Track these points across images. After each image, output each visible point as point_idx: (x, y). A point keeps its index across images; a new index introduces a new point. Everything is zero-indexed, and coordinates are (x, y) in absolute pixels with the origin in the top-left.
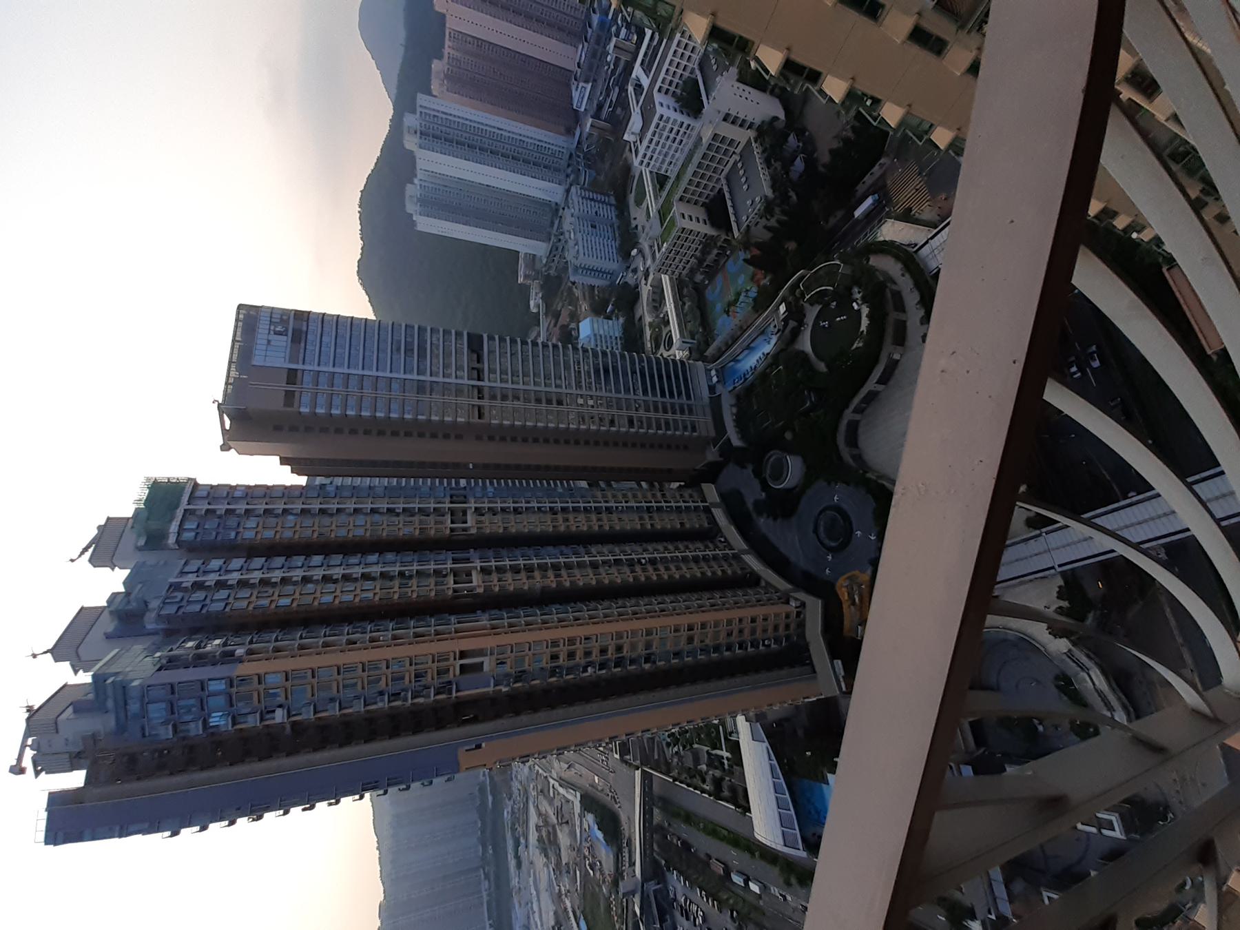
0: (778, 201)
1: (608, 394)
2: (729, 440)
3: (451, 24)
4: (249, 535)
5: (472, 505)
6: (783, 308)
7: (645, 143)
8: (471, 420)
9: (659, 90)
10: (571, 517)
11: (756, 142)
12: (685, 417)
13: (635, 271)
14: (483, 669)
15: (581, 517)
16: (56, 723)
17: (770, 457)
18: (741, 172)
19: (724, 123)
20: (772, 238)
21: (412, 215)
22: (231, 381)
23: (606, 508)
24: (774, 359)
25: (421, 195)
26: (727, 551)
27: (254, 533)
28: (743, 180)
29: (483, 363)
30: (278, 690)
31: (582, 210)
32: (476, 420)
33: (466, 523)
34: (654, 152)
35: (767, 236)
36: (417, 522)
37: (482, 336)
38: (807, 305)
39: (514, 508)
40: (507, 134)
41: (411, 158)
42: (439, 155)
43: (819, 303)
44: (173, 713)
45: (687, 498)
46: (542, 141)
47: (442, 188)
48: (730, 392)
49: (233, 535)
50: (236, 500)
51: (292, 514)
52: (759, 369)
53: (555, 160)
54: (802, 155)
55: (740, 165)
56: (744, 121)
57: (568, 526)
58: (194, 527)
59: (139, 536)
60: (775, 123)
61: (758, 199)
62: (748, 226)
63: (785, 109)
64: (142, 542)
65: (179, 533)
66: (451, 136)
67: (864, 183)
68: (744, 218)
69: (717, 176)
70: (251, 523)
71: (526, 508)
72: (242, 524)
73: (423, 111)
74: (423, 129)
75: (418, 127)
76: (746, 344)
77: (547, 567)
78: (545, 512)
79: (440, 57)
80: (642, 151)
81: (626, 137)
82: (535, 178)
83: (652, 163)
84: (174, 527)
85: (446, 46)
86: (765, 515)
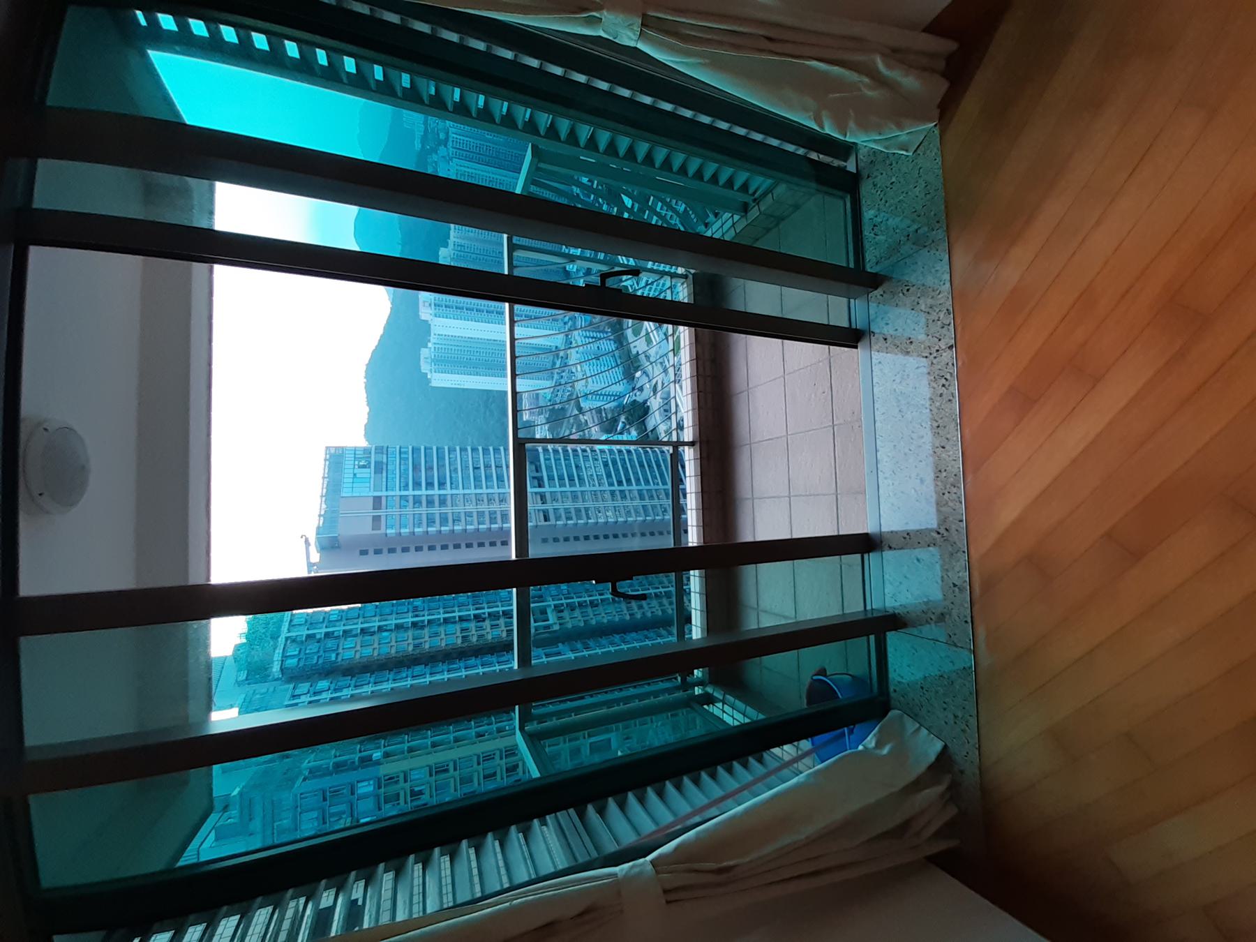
1: (656, 487)
4: (349, 655)
8: (539, 524)
13: (641, 389)
14: (610, 747)
16: (198, 851)
21: (427, 374)
22: (323, 513)
25: (435, 356)
27: (353, 652)
30: (423, 787)
36: (503, 625)
41: (426, 326)
42: (452, 320)
44: (324, 823)
49: (333, 656)
51: (386, 631)
58: (296, 653)
59: (239, 670)
64: (243, 676)
65: (282, 661)
66: (461, 305)
70: (349, 643)
72: (341, 645)
74: (436, 302)
75: (433, 301)
79: (446, 246)
82: (537, 328)
84: (277, 656)
85: (451, 237)
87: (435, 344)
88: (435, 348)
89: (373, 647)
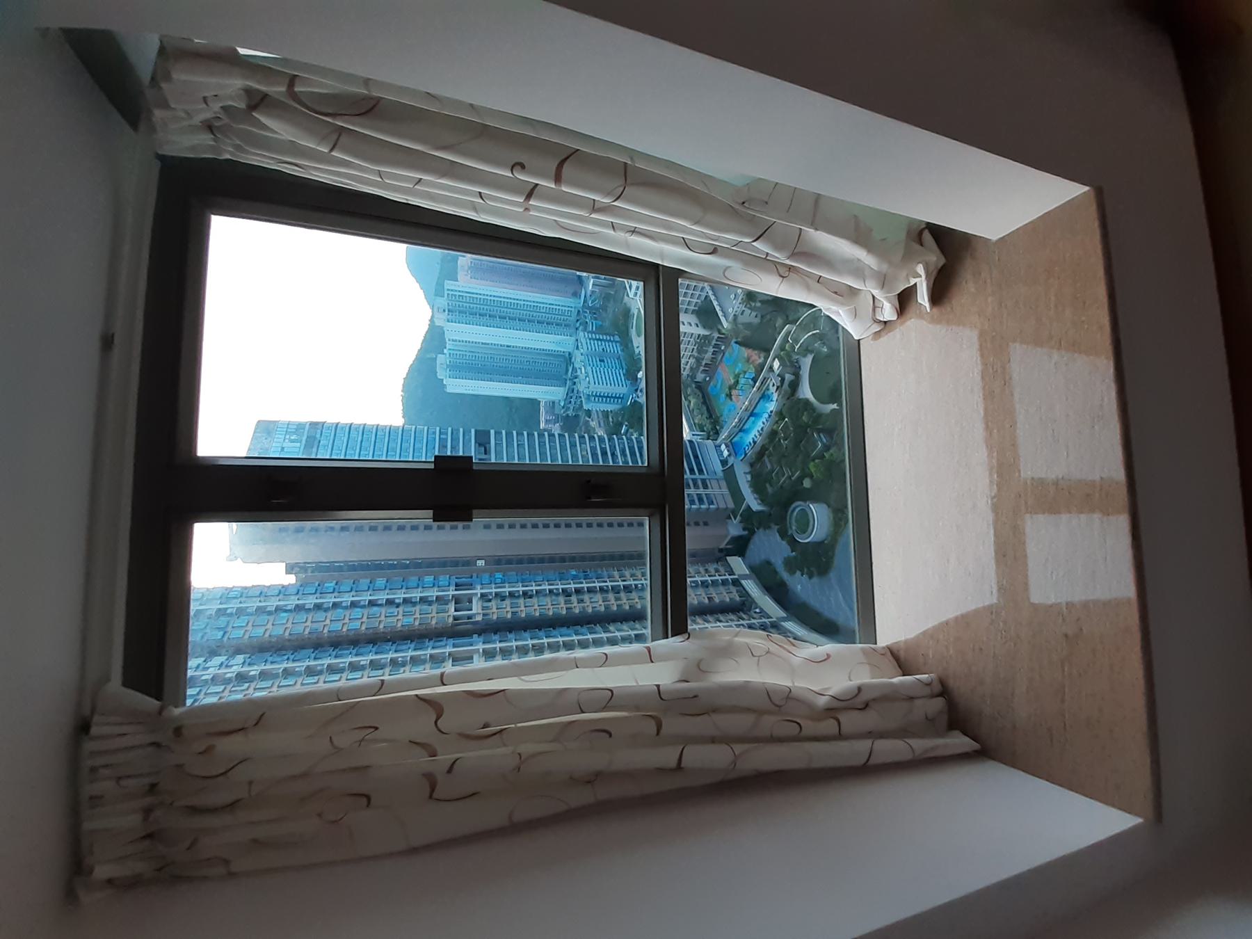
2: (749, 507)
5: (478, 591)
6: (776, 364)
10: (586, 597)
15: (598, 597)
21: (443, 380)
23: (624, 586)
24: (780, 415)
25: (450, 362)
26: (764, 620)
29: (490, 454)
31: (590, 349)
33: (471, 610)
37: (489, 432)
39: (523, 591)
40: (522, 303)
45: (713, 572)
46: (553, 305)
47: (468, 354)
48: (742, 460)
50: (229, 599)
53: (565, 318)
57: (584, 608)
62: (735, 315)
68: (730, 310)
71: (537, 591)
73: (449, 292)
74: (450, 307)
77: (559, 646)
78: (558, 595)
86: (798, 573)
87: (450, 349)
88: (450, 354)
89: (286, 626)
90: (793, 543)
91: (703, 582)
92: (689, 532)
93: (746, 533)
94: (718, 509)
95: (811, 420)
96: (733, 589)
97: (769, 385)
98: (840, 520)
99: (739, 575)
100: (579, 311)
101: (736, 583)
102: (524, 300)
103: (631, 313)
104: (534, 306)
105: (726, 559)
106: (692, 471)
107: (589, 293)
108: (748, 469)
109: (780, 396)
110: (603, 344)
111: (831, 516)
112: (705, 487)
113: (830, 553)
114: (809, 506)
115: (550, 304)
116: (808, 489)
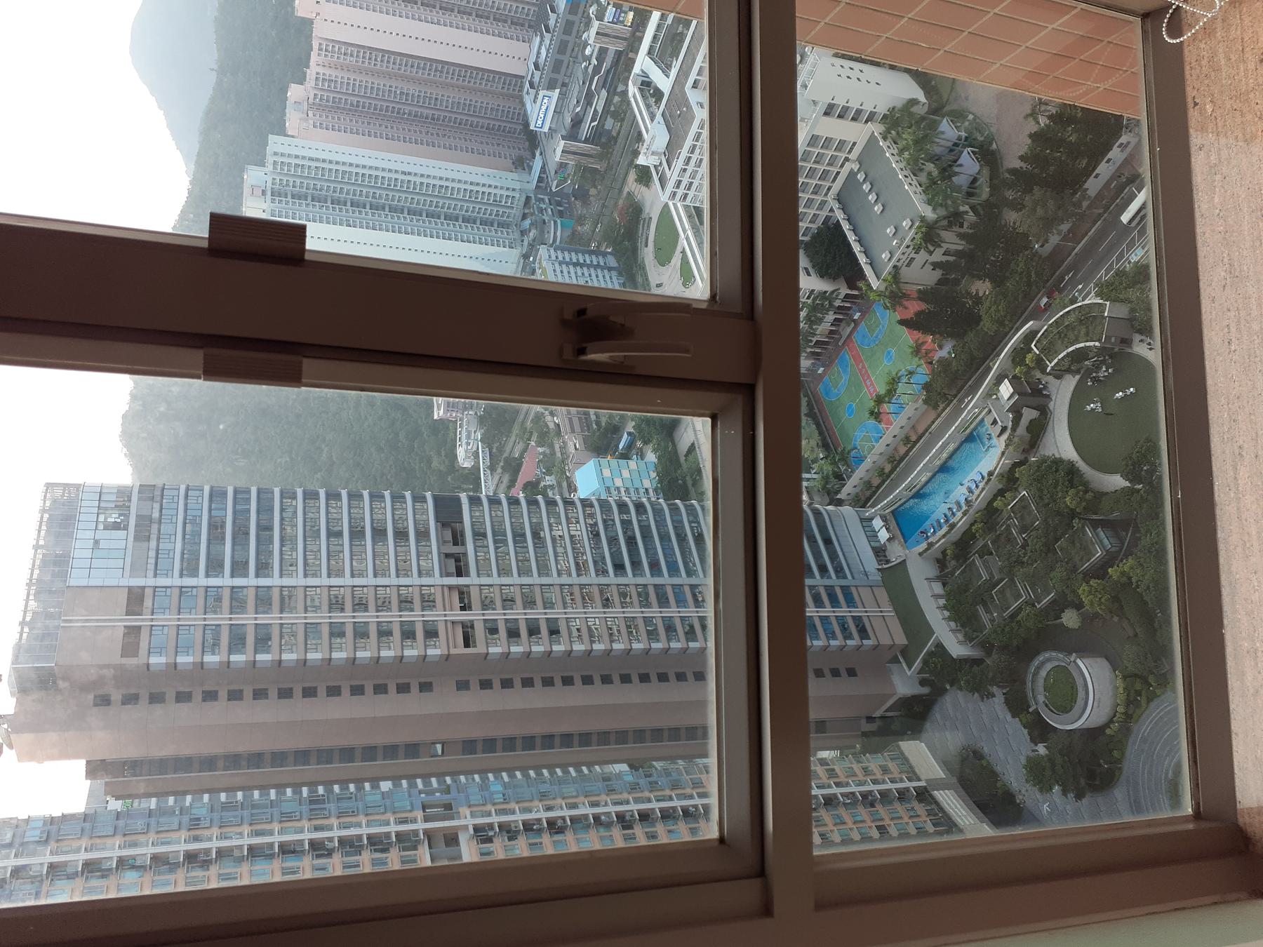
0: (945, 223)
2: (939, 646)
3: (321, 31)
6: (1006, 389)
7: (679, 164)
9: (695, 86)
11: (885, 138)
12: (843, 611)
17: (1038, 668)
18: (866, 187)
19: (826, 119)
20: (940, 282)
24: (1009, 480)
28: (872, 198)
32: (462, 650)
34: (693, 176)
35: (932, 277)
38: (1050, 378)
43: (1074, 373)
52: (979, 504)
54: (969, 149)
55: (861, 177)
56: (859, 112)
60: (915, 109)
61: (906, 224)
62: (895, 267)
63: (923, 88)
67: (1096, 176)
69: (819, 198)
76: (938, 463)
79: (301, 80)
80: (672, 176)
81: (641, 160)
83: (691, 194)
86: (1056, 788)
90: (1040, 730)
91: (865, 795)
92: (815, 688)
93: (925, 690)
94: (875, 648)
95: (1084, 504)
96: (920, 809)
97: (983, 420)
98: (1139, 693)
99: (927, 781)
100: (528, 198)
101: (924, 795)
102: (422, 176)
103: (644, 216)
104: (441, 186)
105: (899, 747)
106: (823, 569)
107: (552, 168)
108: (932, 571)
109: (1011, 448)
110: (587, 274)
111: (1120, 683)
112: (850, 602)
113: (1115, 753)
114: (1075, 662)
115: (472, 183)
116: (1067, 630)
